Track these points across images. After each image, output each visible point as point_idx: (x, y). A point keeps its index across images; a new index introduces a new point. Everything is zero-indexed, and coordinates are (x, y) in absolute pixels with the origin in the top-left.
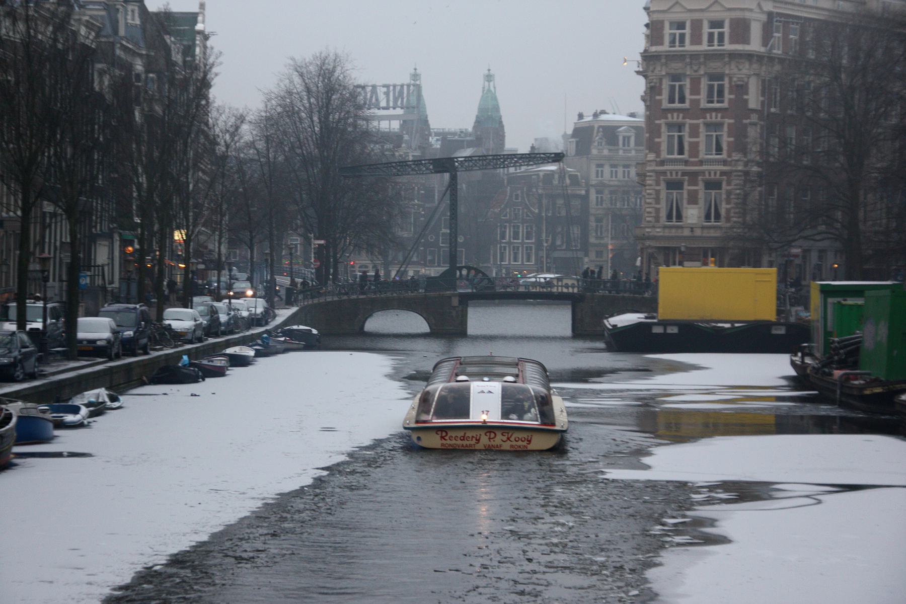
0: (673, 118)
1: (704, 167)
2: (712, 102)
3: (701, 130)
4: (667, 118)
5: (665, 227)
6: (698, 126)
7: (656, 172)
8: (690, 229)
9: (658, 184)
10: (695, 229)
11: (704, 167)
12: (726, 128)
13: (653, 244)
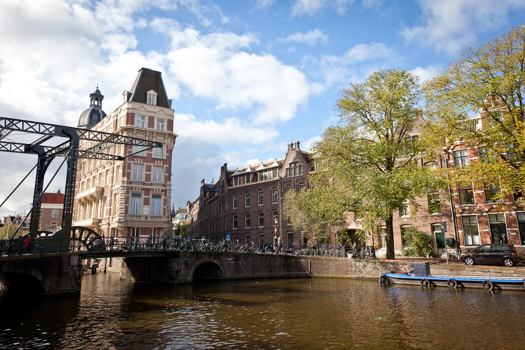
1: (153, 187)
3: (152, 169)
10: (147, 218)
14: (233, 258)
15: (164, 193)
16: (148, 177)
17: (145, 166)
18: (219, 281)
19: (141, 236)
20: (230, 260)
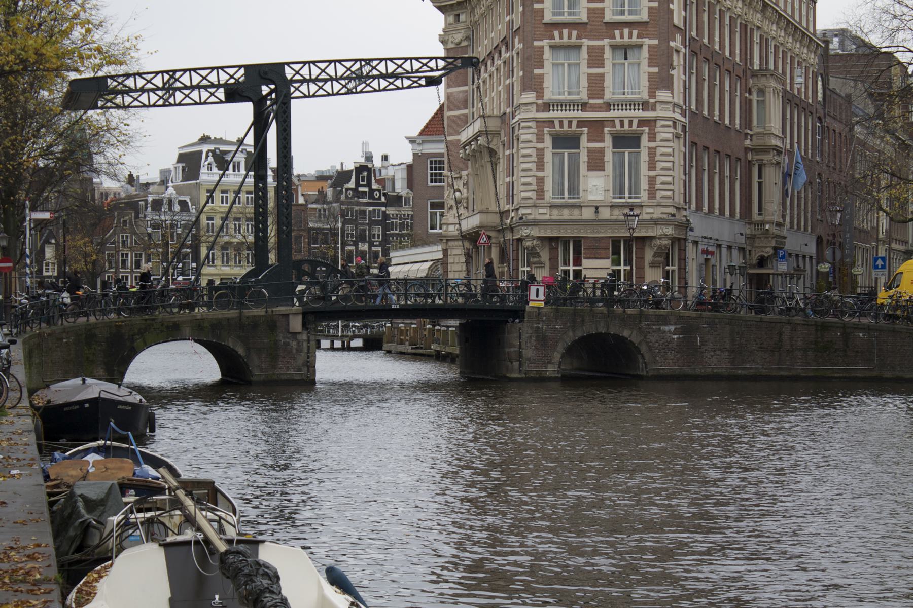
0: (561, 37)
1: (612, 114)
2: (622, 13)
3: (606, 56)
4: (553, 38)
5: (552, 206)
6: (601, 49)
7: (538, 121)
8: (594, 209)
9: (540, 139)
10: (600, 209)
11: (612, 114)
12: (645, 52)
13: (535, 232)
14: (678, 327)
15: (646, 129)
16: (596, 85)
17: (584, 50)
18: (640, 378)
19: (586, 263)
20: (669, 331)
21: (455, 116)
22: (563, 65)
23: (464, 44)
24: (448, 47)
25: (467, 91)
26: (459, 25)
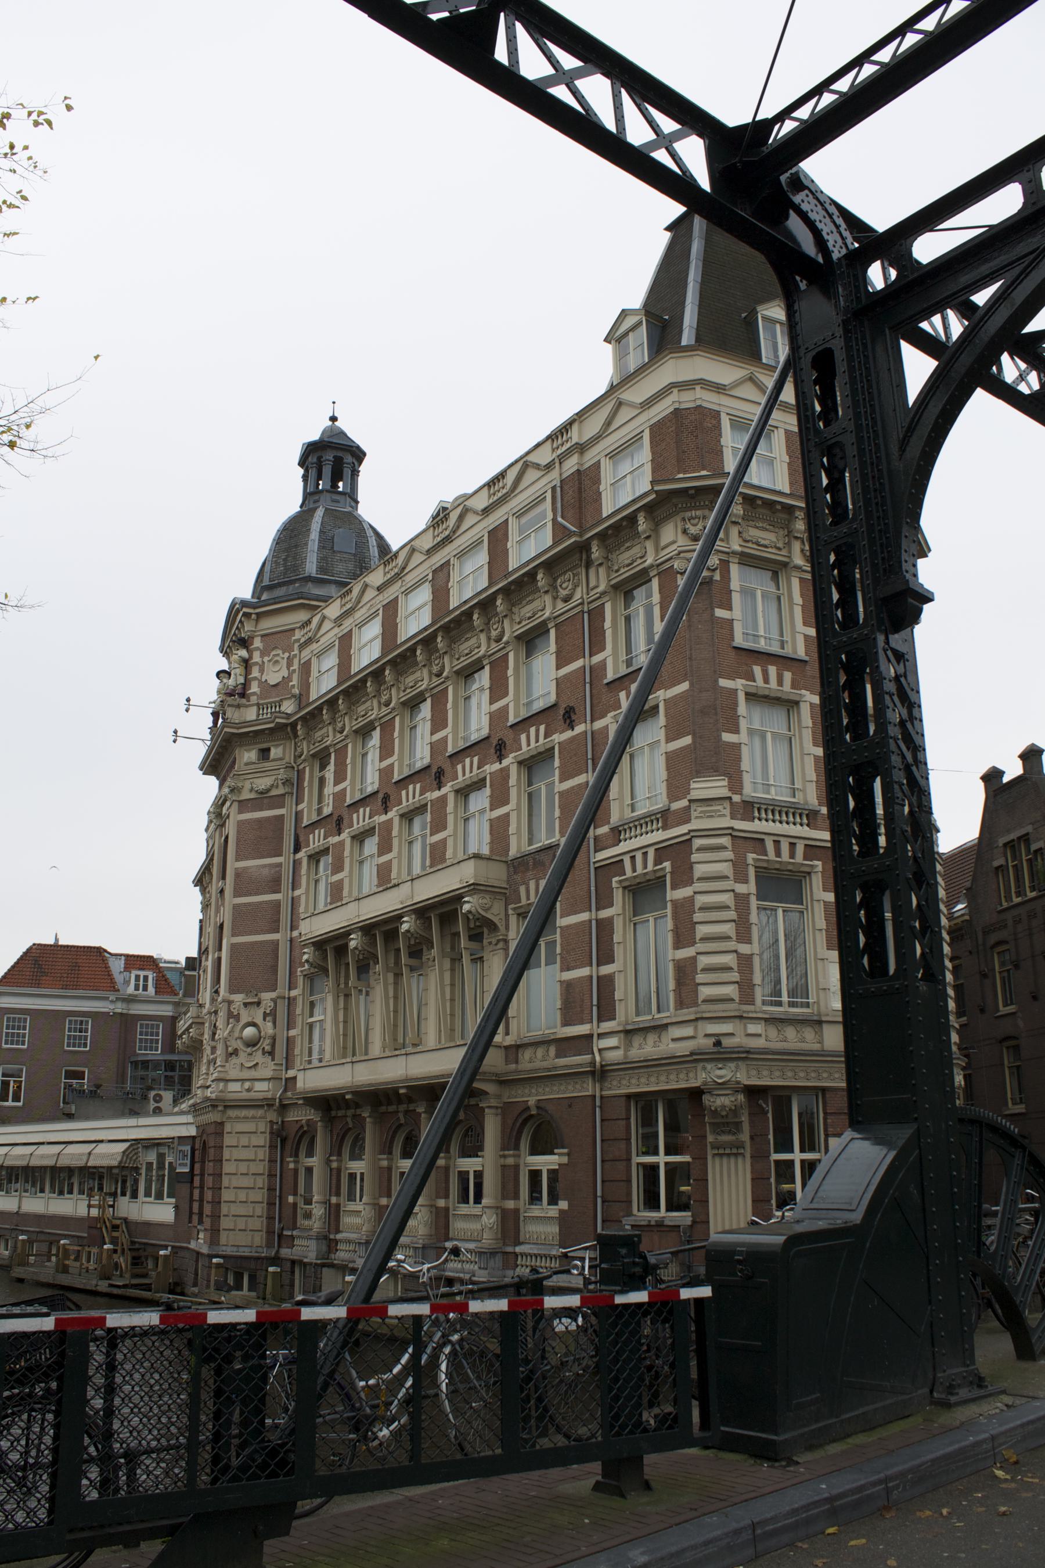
9: (741, 877)
21: (249, 904)
22: (763, 736)
23: (280, 791)
24: (242, 798)
25: (280, 865)
26: (266, 764)
